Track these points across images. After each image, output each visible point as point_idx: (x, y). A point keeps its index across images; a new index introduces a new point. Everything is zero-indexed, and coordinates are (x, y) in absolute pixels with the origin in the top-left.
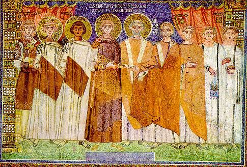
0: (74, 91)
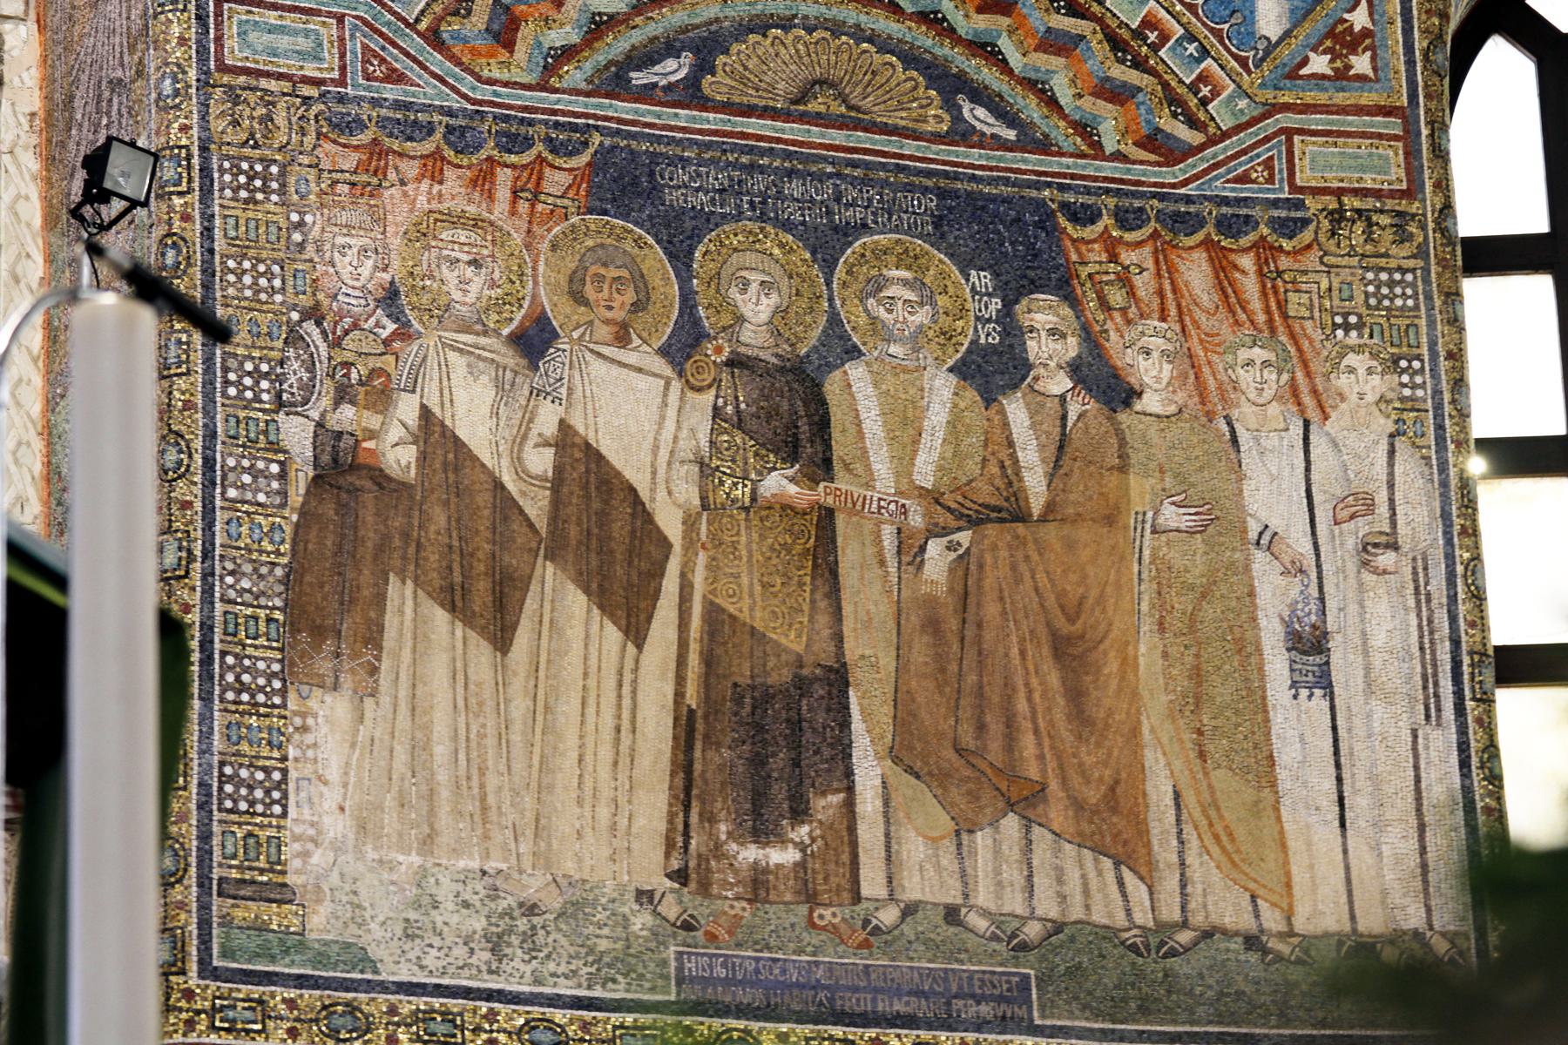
0: (596, 611)
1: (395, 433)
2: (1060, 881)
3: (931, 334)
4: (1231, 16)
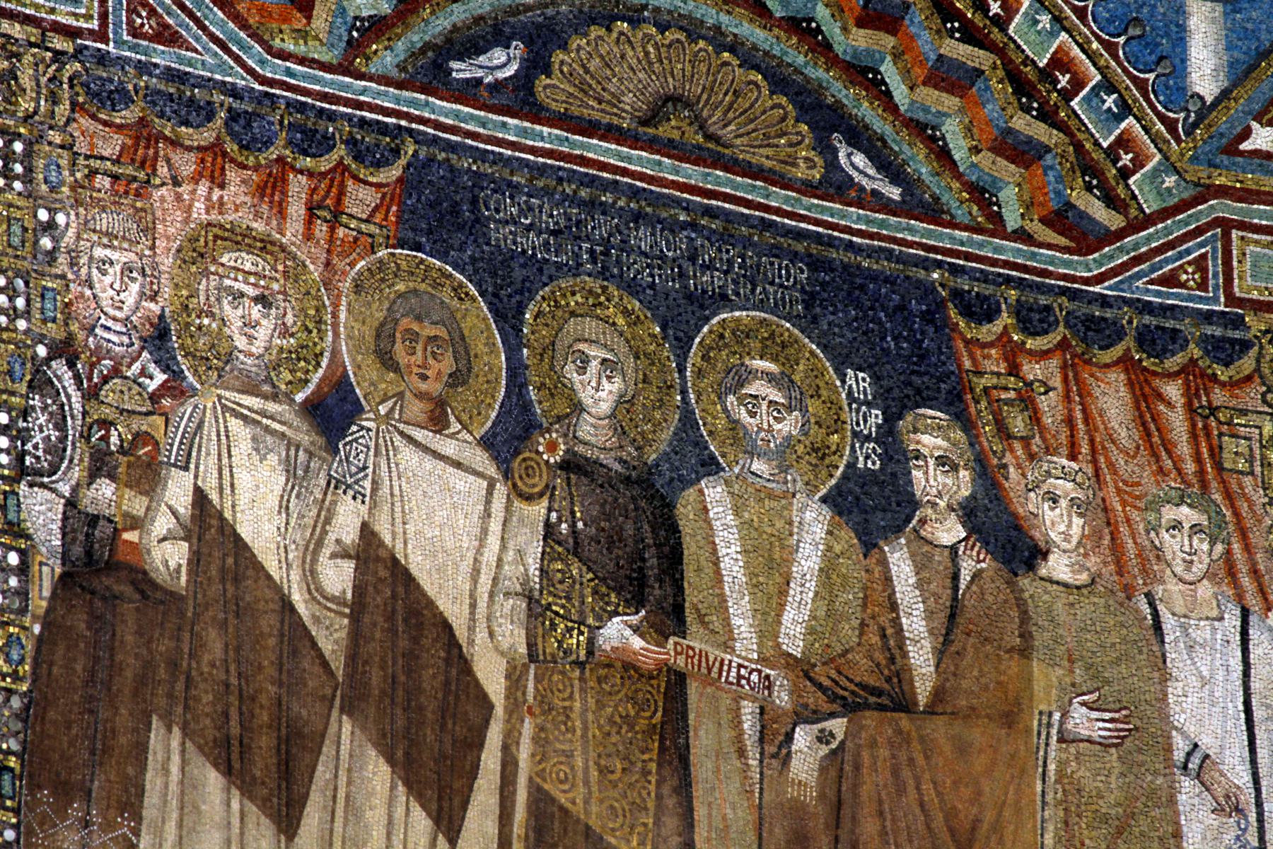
0: (401, 788)
1: (163, 523)
3: (800, 449)
4: (1158, 63)
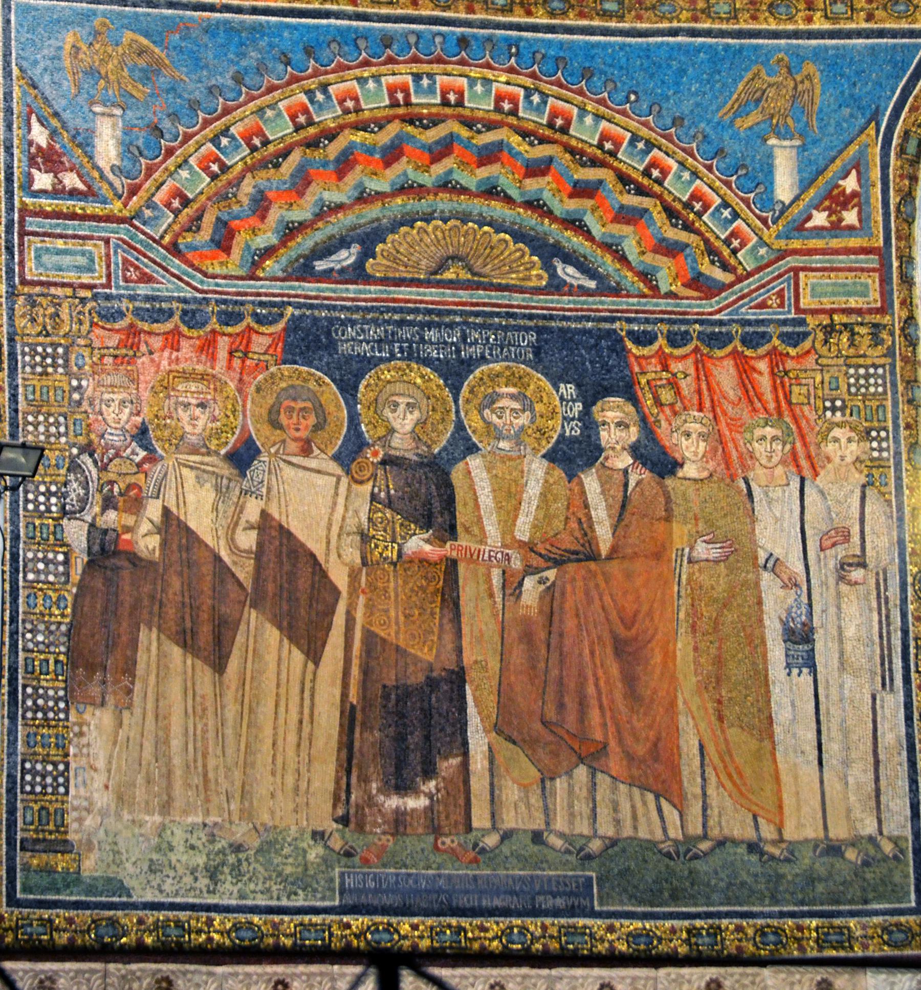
0: (286, 641)
2: (616, 810)
3: (530, 431)
